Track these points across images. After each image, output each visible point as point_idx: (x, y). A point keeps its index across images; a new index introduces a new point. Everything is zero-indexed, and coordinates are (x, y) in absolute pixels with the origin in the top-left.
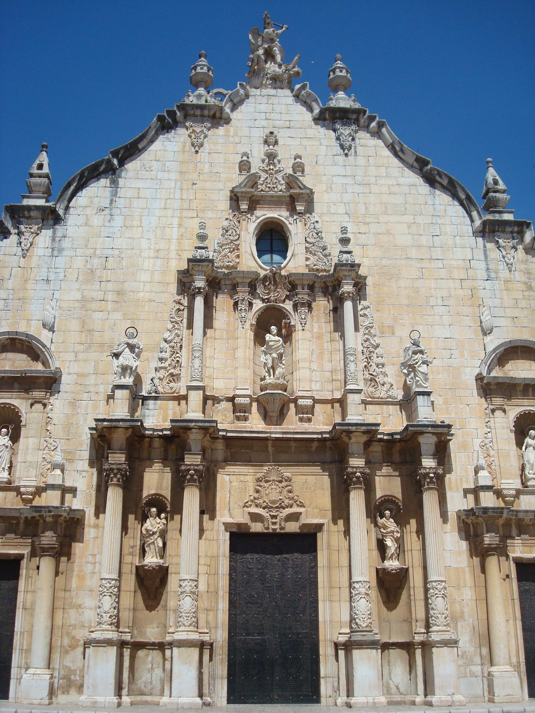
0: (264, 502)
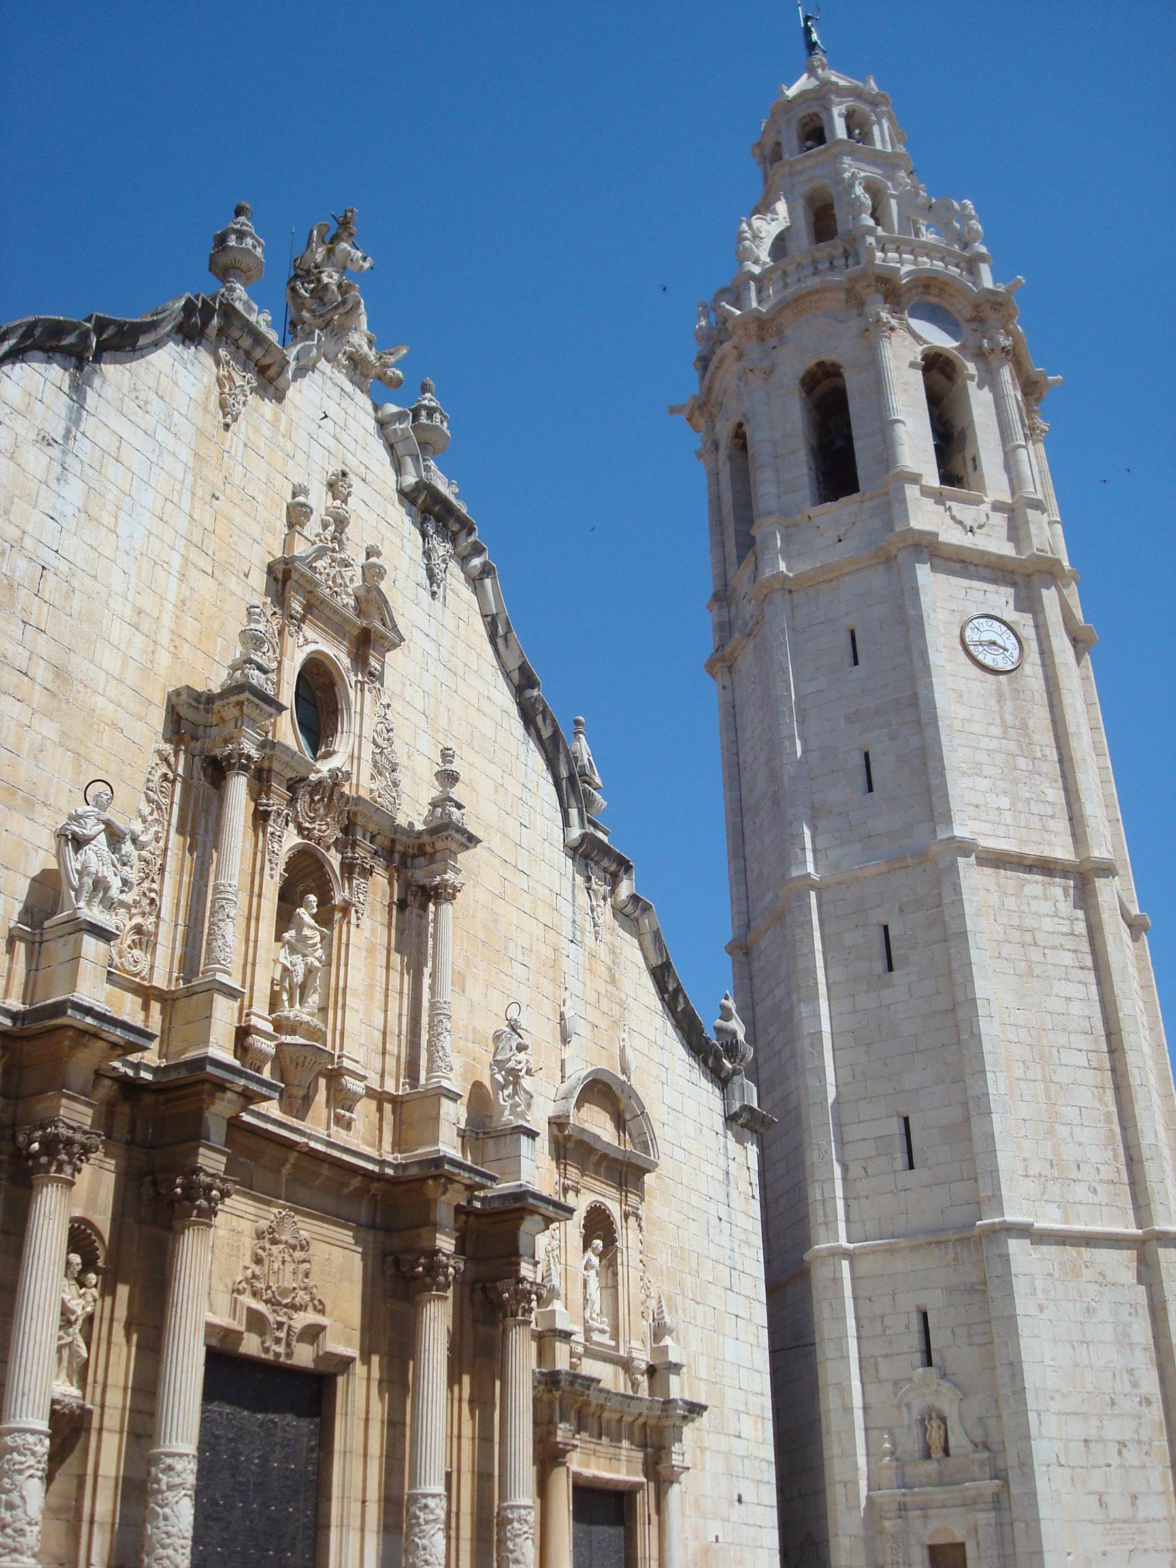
0: (269, 1287)
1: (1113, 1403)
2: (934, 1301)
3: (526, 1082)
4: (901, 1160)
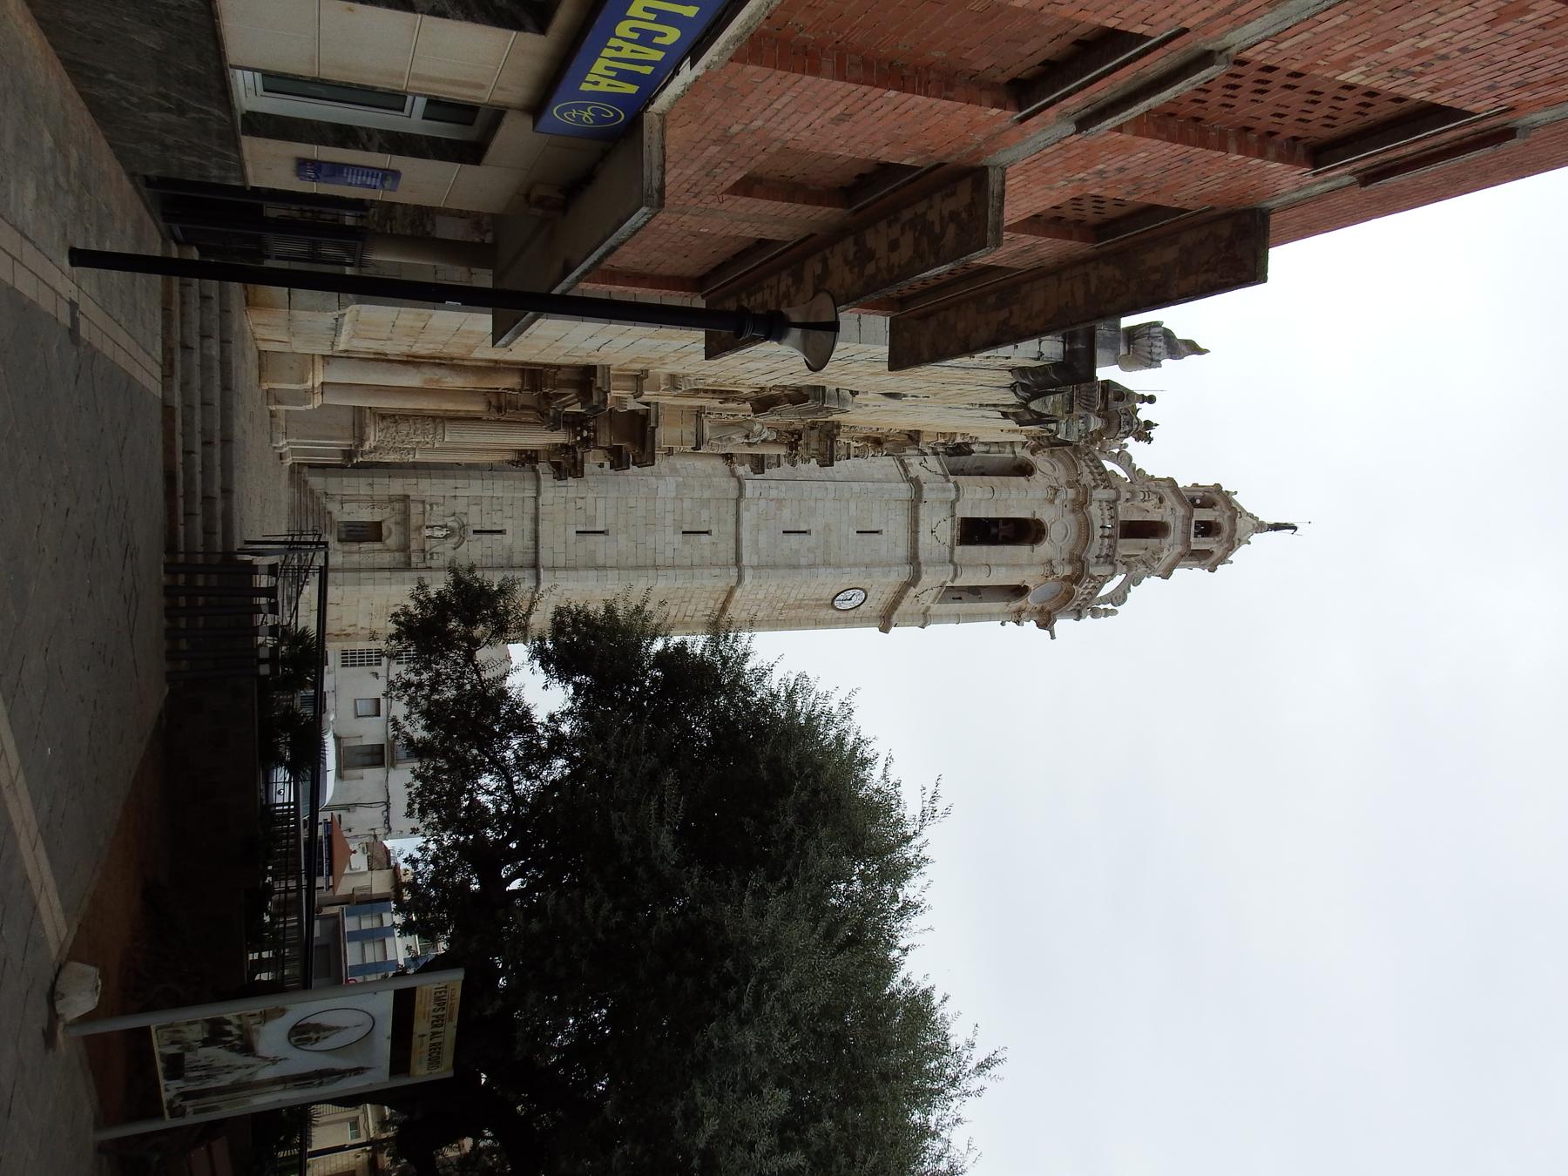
2: (507, 539)
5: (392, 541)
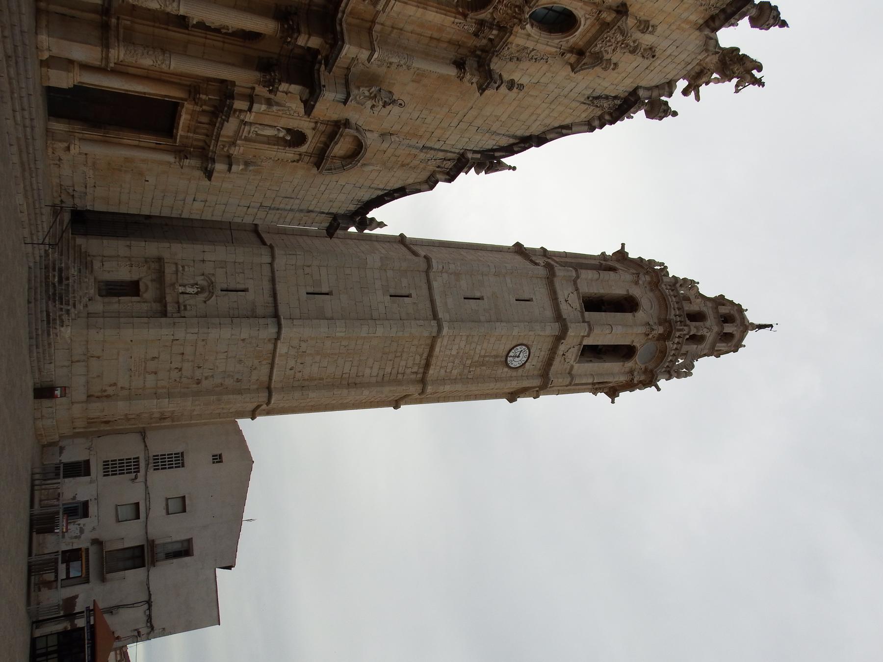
1: (199, 367)
2: (250, 296)
3: (369, 103)
4: (311, 290)
5: (149, 293)
